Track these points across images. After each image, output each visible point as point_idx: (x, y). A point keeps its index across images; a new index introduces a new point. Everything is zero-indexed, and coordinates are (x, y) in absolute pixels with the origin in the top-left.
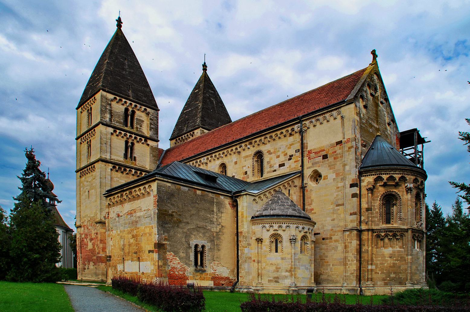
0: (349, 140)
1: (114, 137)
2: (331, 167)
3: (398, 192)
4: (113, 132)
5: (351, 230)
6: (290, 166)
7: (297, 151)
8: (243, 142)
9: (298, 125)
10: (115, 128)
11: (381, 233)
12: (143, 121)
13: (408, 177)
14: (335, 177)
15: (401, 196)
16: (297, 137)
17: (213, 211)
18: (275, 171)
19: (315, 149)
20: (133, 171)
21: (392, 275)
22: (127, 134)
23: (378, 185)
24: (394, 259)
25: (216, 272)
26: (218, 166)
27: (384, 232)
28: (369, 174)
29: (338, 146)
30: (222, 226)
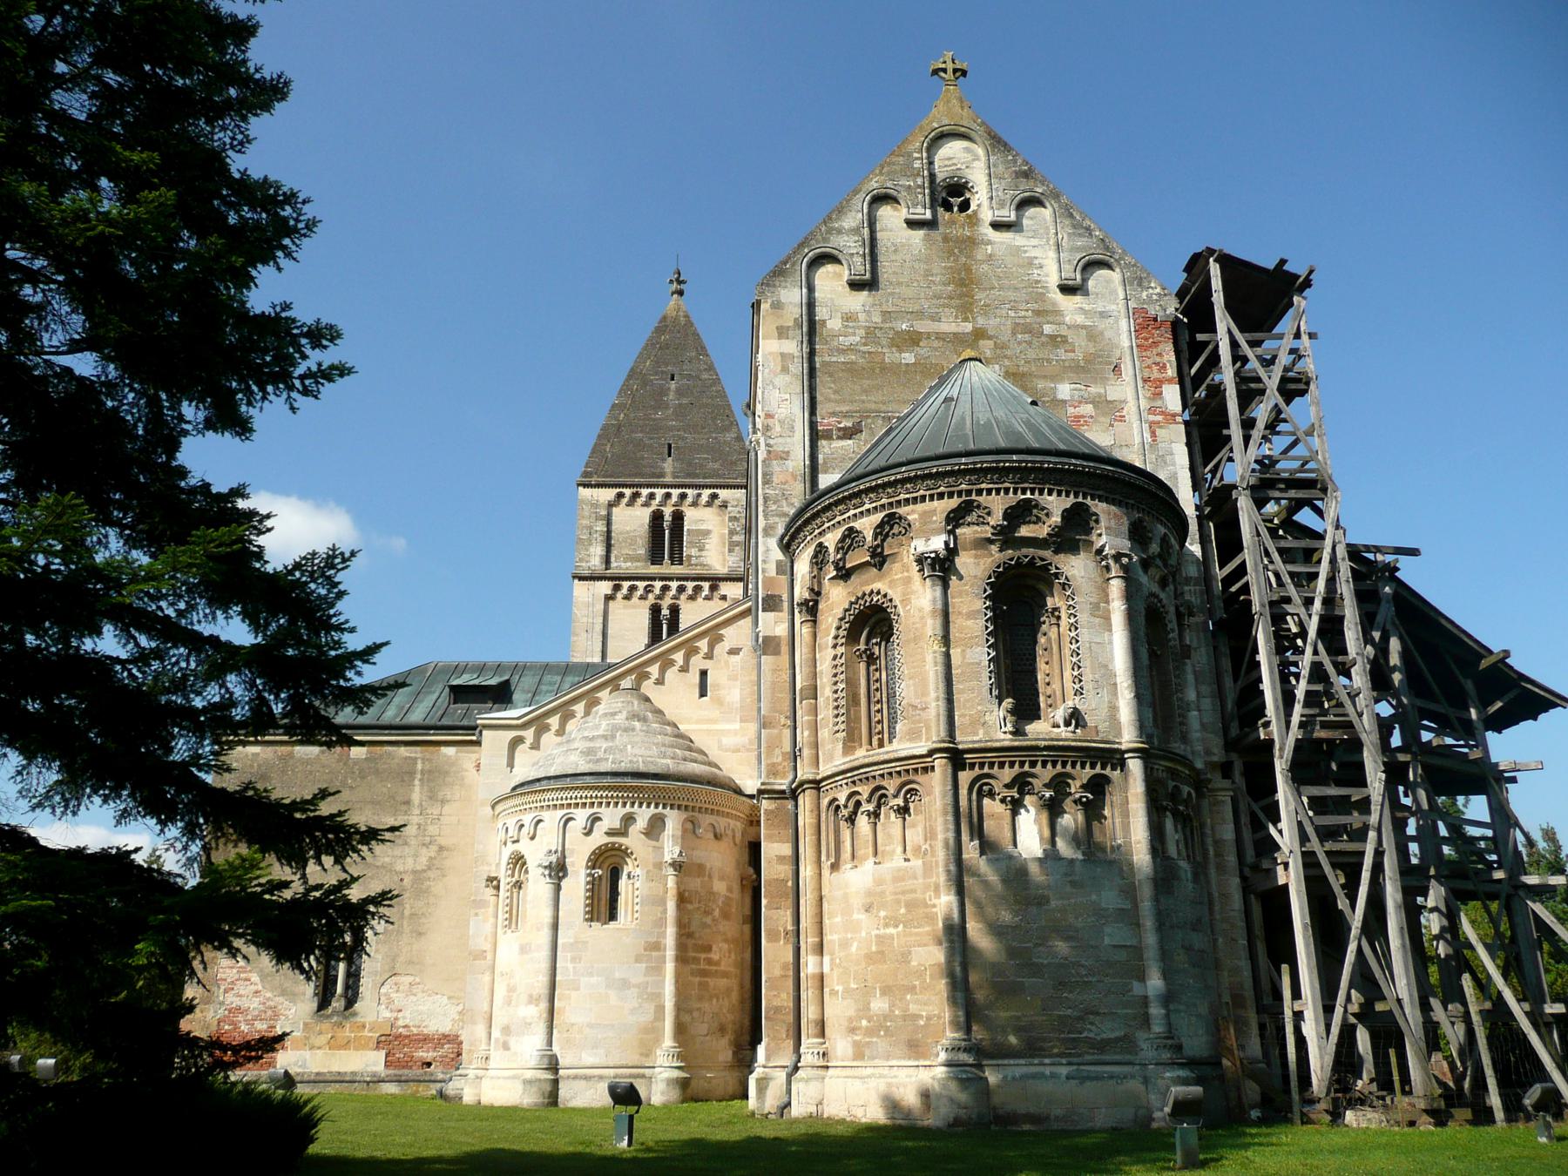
3: (890, 587)
10: (617, 579)
12: (707, 533)
13: (912, 513)
17: (408, 803)
30: (441, 848)
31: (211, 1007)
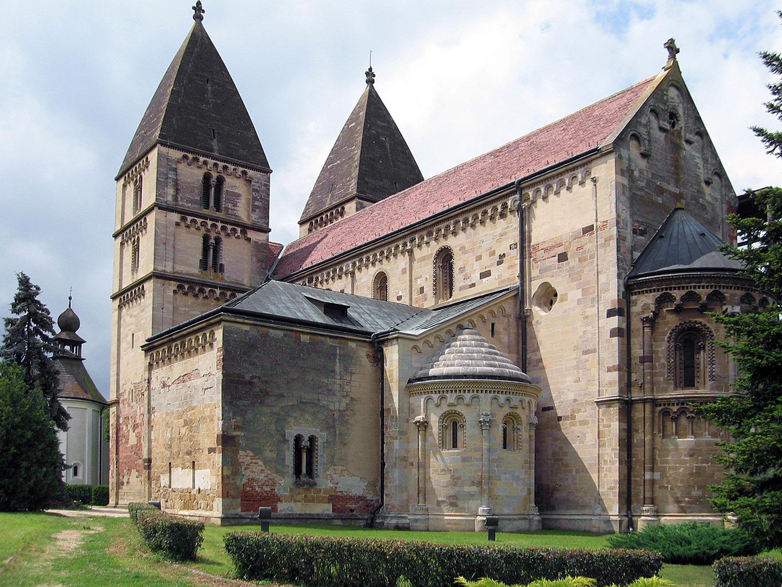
0: (605, 224)
1: (182, 230)
2: (574, 276)
3: (708, 322)
5: (608, 403)
6: (500, 276)
7: (513, 246)
8: (417, 231)
9: (514, 196)
10: (184, 213)
11: (671, 407)
12: (238, 196)
13: (727, 293)
14: (580, 297)
15: (713, 330)
16: (514, 220)
18: (473, 285)
19: (545, 242)
20: (218, 291)
21: (696, 493)
23: (665, 310)
24: (700, 458)
25: (338, 486)
26: (372, 279)
27: (678, 404)
28: (646, 289)
29: (587, 236)
31: (239, 478)
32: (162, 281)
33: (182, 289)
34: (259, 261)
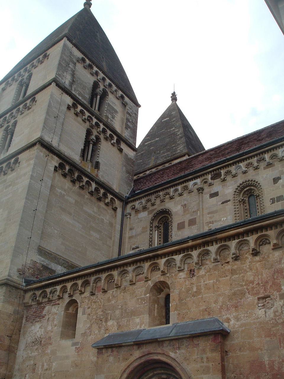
4: (71, 105)
12: (116, 112)
22: (92, 119)
32: (47, 152)
33: (62, 170)
34: (128, 172)
